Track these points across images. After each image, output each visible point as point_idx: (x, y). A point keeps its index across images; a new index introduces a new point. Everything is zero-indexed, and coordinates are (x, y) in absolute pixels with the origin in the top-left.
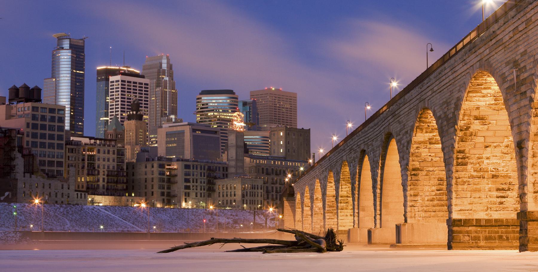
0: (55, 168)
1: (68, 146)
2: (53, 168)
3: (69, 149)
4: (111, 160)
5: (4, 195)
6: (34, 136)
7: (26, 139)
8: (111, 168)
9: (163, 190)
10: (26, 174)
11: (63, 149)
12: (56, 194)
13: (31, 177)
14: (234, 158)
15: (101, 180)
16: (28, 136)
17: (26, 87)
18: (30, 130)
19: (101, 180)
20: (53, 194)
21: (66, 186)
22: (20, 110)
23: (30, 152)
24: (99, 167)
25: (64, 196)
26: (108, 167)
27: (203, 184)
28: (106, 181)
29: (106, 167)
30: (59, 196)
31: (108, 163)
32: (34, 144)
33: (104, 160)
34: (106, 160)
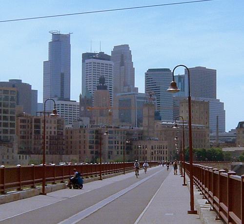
0: (9, 135)
2: (7, 135)
8: (53, 134)
9: (92, 150)
14: (147, 125)
28: (49, 143)
31: (50, 130)
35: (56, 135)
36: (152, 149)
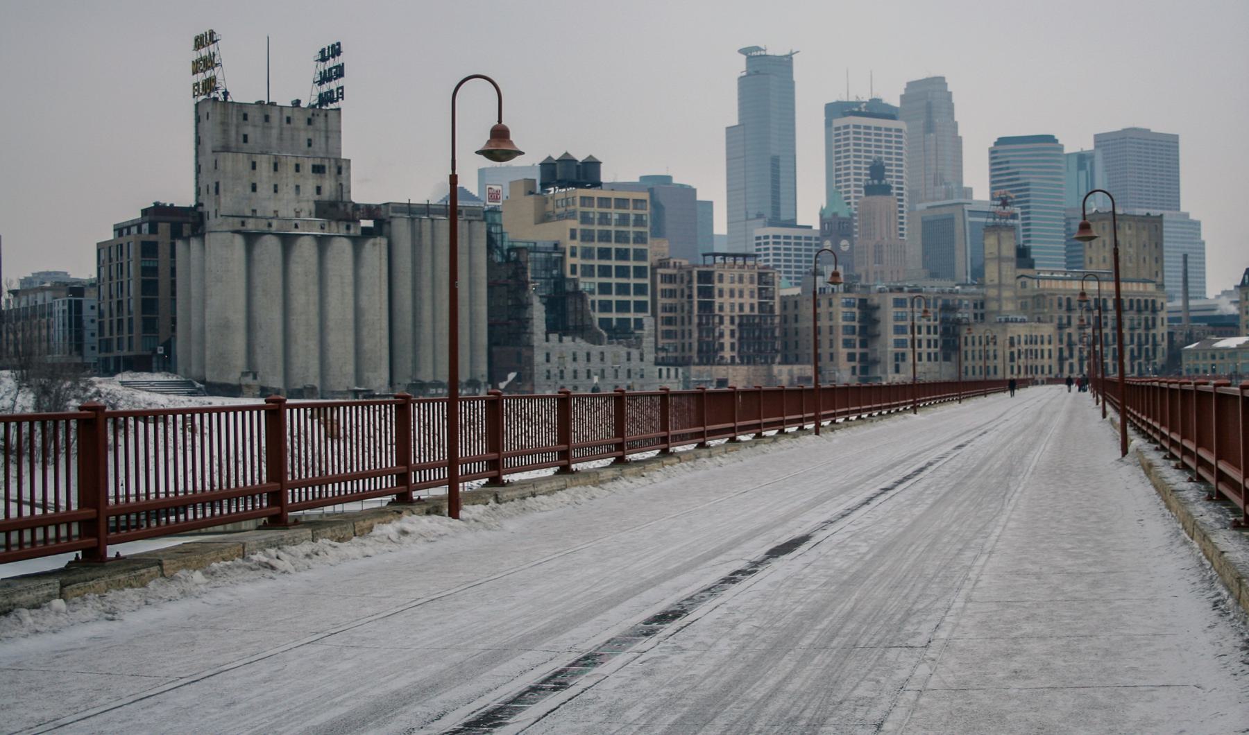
0: (632, 315)
1: (660, 271)
2: (626, 316)
3: (662, 275)
4: (746, 293)
5: (506, 379)
6: (587, 253)
7: (570, 261)
8: (747, 310)
9: (851, 350)
10: (551, 336)
11: (646, 277)
12: (616, 371)
13: (561, 341)
14: (996, 282)
15: (727, 333)
16: (573, 254)
17: (567, 160)
18: (577, 243)
19: (727, 333)
20: (609, 373)
21: (635, 353)
22: (559, 203)
23: (576, 286)
24: (721, 308)
25: (632, 375)
26: (741, 307)
27: (933, 336)
28: (737, 335)
29: (737, 308)
30: (622, 374)
32: (588, 271)
33: (732, 294)
34: (737, 294)
35: (756, 312)
36: (1012, 344)
